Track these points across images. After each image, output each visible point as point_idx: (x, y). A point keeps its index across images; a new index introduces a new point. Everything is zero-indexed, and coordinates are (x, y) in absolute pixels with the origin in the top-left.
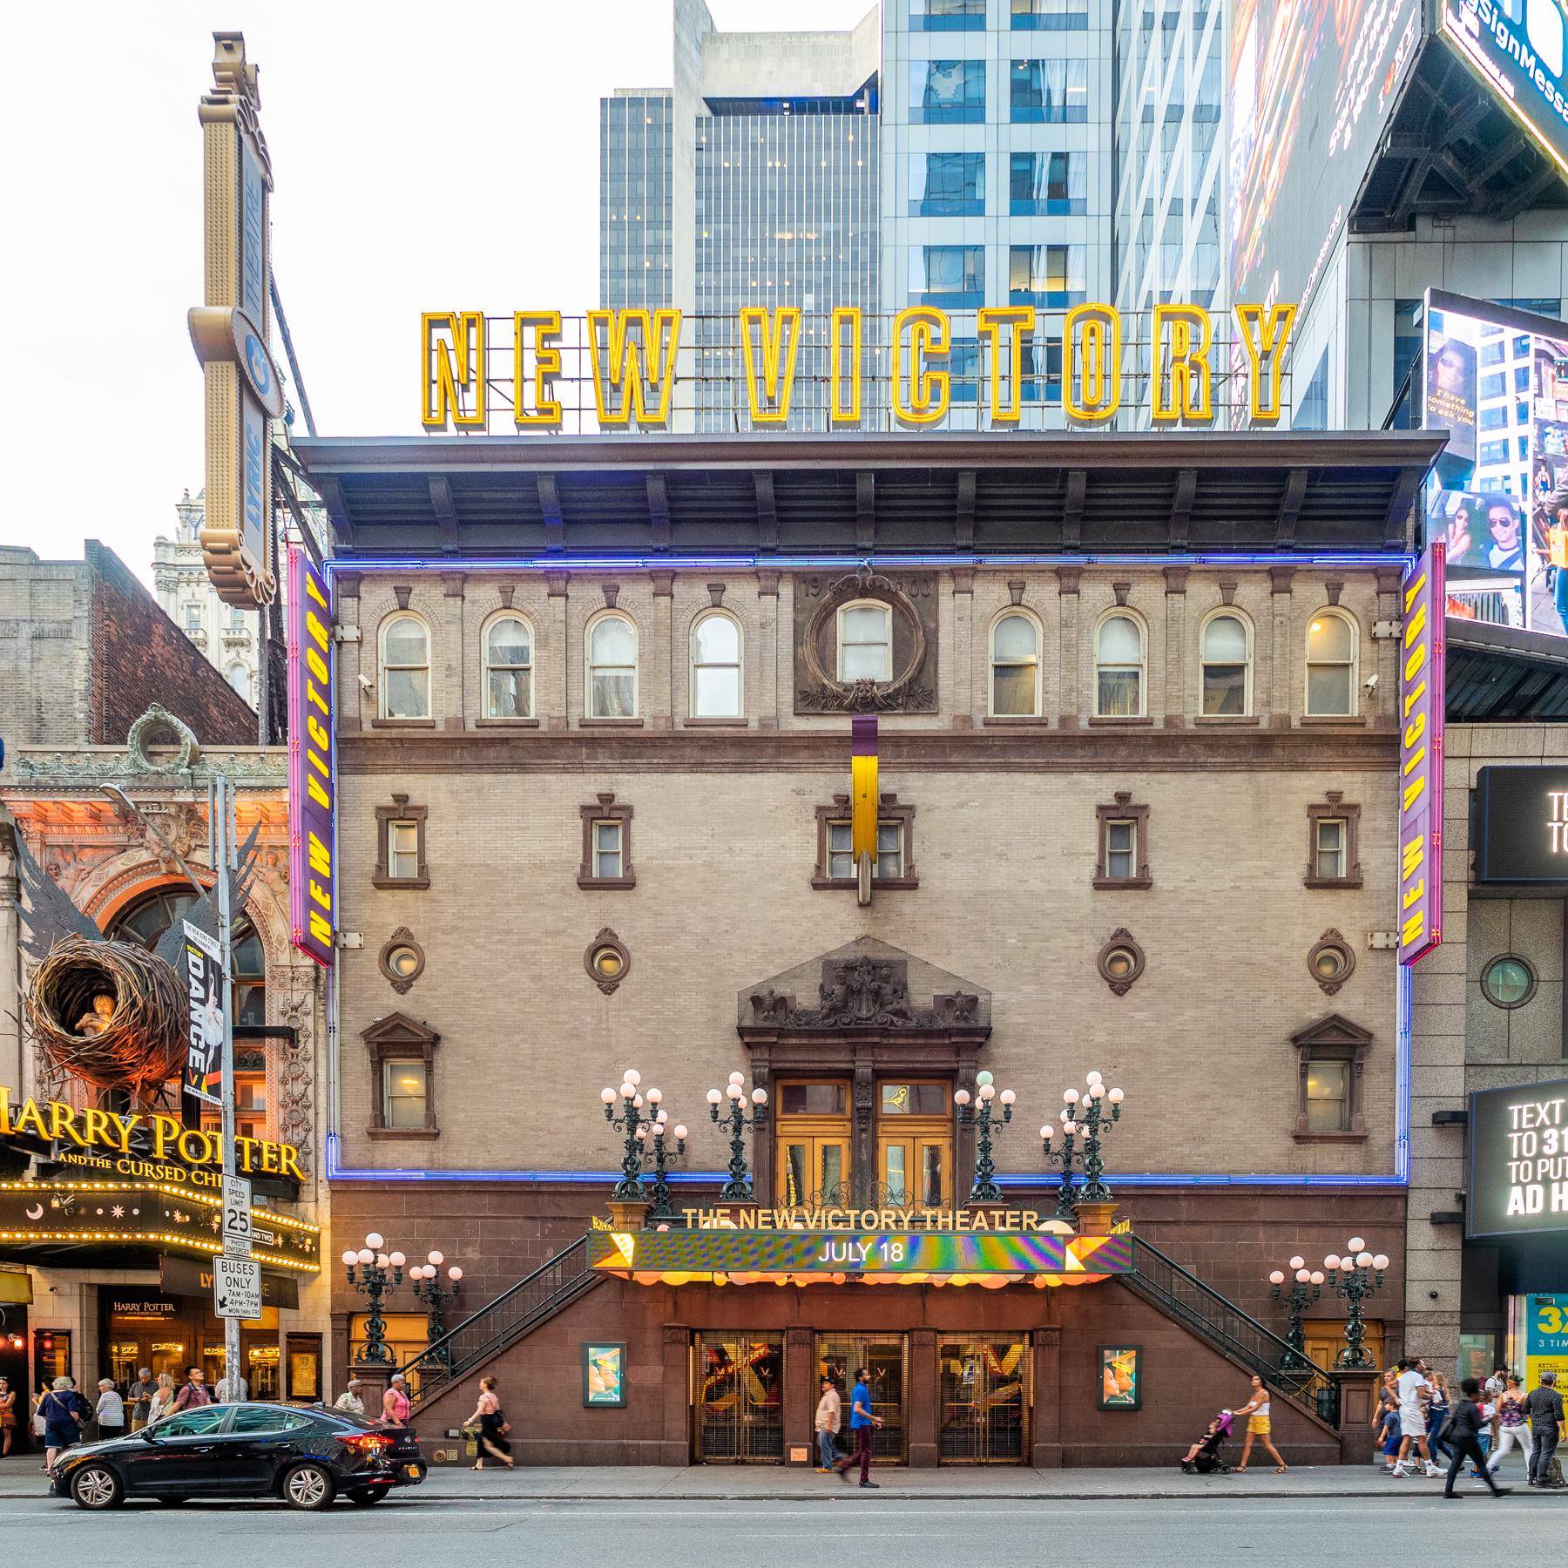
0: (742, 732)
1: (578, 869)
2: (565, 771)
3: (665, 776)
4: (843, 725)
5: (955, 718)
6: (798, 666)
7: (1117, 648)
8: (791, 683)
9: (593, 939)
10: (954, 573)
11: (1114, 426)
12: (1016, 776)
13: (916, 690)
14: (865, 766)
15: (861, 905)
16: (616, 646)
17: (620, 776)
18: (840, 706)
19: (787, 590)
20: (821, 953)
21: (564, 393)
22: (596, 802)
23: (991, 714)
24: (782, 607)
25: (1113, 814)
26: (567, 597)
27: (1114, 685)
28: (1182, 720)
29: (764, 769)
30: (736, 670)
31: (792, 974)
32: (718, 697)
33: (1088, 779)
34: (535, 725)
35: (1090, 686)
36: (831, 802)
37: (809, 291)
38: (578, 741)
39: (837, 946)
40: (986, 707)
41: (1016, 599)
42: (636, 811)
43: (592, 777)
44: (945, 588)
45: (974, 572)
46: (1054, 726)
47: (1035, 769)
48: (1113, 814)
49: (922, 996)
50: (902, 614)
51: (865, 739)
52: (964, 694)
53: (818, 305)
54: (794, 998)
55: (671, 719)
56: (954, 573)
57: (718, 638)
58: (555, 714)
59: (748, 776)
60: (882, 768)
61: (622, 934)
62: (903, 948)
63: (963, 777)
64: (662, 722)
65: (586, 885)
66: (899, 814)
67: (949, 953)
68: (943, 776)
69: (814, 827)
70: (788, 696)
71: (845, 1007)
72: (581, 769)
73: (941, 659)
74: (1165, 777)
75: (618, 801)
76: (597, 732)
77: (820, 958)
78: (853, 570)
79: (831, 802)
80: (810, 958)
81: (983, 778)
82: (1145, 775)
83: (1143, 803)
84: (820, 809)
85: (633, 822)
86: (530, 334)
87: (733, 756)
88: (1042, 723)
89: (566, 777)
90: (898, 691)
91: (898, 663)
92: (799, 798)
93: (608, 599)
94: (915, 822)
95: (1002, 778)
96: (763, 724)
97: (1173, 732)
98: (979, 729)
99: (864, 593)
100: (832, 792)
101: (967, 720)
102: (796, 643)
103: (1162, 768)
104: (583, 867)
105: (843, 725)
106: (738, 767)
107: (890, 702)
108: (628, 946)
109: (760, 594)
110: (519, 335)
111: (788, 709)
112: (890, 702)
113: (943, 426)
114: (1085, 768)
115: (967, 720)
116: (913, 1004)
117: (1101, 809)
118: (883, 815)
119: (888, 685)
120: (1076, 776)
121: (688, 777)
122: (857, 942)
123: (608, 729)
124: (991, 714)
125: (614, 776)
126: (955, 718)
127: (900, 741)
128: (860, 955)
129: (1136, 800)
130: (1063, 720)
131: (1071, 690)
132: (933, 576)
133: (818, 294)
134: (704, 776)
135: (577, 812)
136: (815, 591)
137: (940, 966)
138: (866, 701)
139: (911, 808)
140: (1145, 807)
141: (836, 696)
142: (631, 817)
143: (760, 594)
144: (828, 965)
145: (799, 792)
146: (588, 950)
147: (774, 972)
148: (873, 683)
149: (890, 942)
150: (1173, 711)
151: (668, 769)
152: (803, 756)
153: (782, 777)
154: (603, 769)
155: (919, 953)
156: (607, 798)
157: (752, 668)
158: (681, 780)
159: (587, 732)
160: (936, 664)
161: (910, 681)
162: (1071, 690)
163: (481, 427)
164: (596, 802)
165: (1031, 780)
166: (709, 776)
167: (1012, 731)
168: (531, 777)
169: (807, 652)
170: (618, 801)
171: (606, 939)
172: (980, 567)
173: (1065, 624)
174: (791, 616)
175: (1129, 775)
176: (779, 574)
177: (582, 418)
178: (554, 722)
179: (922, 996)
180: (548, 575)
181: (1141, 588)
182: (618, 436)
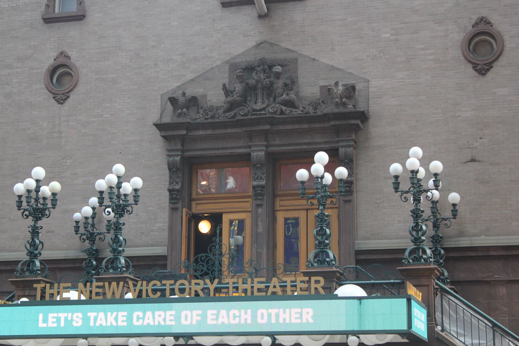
1: (43, 7)
9: (51, 61)
15: (260, 17)
20: (228, 58)
31: (204, 77)
39: (241, 51)
49: (309, 87)
54: (205, 96)
61: (74, 55)
62: (295, 49)
65: (48, 21)
67: (333, 49)
71: (245, 101)
77: (227, 62)
80: (219, 63)
104: (47, 6)
108: (78, 64)
116: (302, 94)
122: (258, 45)
128: (259, 57)
137: (325, 61)
144: (233, 66)
146: (48, 70)
147: (190, 76)
149: (284, 45)
155: (308, 51)
171: (62, 60)
179: (309, 87)
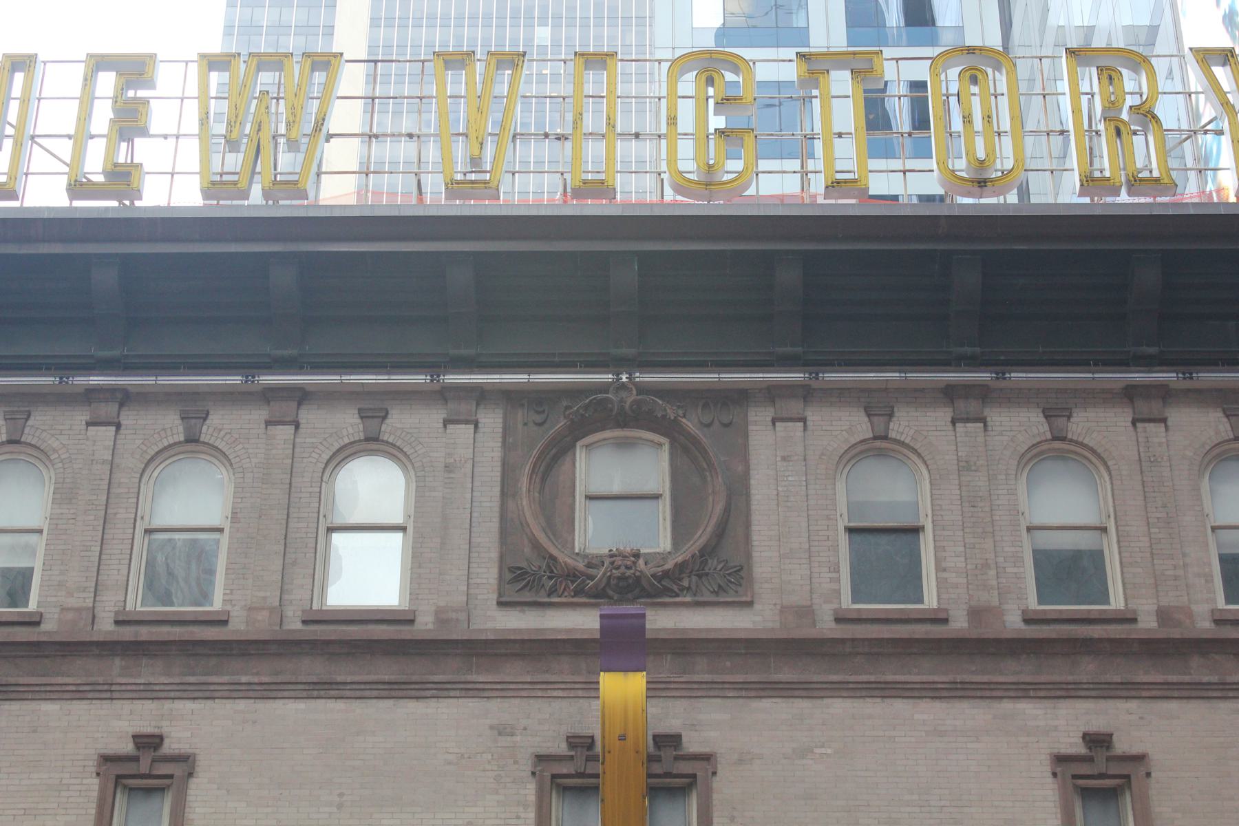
0: (404, 633)
2: (78, 694)
3: (261, 706)
4: (584, 621)
5: (784, 609)
6: (508, 528)
7: (1063, 505)
8: (494, 555)
10: (772, 393)
11: (1024, 192)
12: (900, 706)
13: (713, 565)
14: (623, 688)
16: (193, 500)
17: (180, 706)
18: (577, 593)
19: (492, 420)
21: (146, 152)
22: (128, 748)
23: (846, 602)
24: (481, 445)
25: (1084, 769)
26: (118, 426)
27: (1069, 570)
28: (1190, 614)
29: (441, 691)
30: (398, 537)
32: (367, 575)
33: (1031, 711)
34: (33, 622)
35: (1018, 560)
36: (562, 748)
37: (543, 23)
38: (108, 648)
40: (838, 592)
41: (880, 431)
42: (202, 763)
43: (125, 707)
44: (759, 419)
45: (806, 394)
46: (959, 624)
47: (933, 692)
48: (1084, 769)
50: (687, 452)
51: (622, 645)
52: (798, 564)
53: (556, 45)
55: (279, 612)
56: (772, 393)
57: (373, 487)
58: (72, 602)
59: (412, 705)
60: (654, 690)
63: (803, 705)
64: (263, 616)
66: (685, 767)
68: (766, 704)
69: (530, 791)
70: (488, 574)
72: (105, 692)
73: (756, 518)
74: (1173, 706)
75: (171, 746)
76: (144, 633)
78: (604, 388)
79: (562, 748)
81: (839, 707)
82: (1133, 705)
83: (1136, 750)
84: (541, 759)
85: (193, 783)
86: (107, 82)
87: (386, 670)
88: (939, 619)
89: (79, 707)
90: (681, 567)
91: (681, 526)
92: (505, 741)
93: (187, 430)
94: (716, 783)
95: (872, 708)
96: (442, 619)
97: (1176, 634)
98: (826, 626)
99: (623, 420)
100: (565, 729)
101: (806, 612)
102: (507, 491)
103: (1167, 691)
105: (584, 621)
106: (395, 690)
107: (665, 584)
109: (446, 422)
110: (89, 81)
111: (487, 594)
112: (665, 584)
113: (751, 191)
114: (1024, 691)
115: (806, 612)
117: (1061, 760)
118: (657, 768)
119: (664, 557)
120: (1007, 706)
121: (301, 705)
123: (165, 629)
124: (846, 602)
125: (168, 705)
126: (784, 609)
127: (684, 647)
129: (1122, 746)
130: (976, 614)
131: (986, 565)
132: (740, 397)
133: (556, 26)
134: (332, 704)
135: (92, 766)
136: (539, 418)
138: (625, 583)
139: (707, 758)
140: (1140, 758)
141: (572, 575)
142: (190, 775)
143: (446, 422)
145: (502, 731)
148: (637, 555)
150: (1170, 599)
151: (268, 691)
152: (513, 672)
153: (472, 705)
154: (149, 693)
156: (149, 742)
157: (425, 535)
158: (291, 710)
159: (127, 633)
160: (748, 525)
161: (703, 552)
162: (986, 565)
163: (13, 195)
164: (128, 748)
165: (928, 712)
166: (340, 705)
167: (886, 632)
168: (15, 706)
169: (525, 505)
170: (169, 747)
172: (814, 384)
173: (965, 467)
174: (497, 454)
175: (1103, 704)
176: (481, 395)
177: (172, 180)
178: (70, 616)
180: (90, 396)
181: (1091, 414)
182: (229, 207)
